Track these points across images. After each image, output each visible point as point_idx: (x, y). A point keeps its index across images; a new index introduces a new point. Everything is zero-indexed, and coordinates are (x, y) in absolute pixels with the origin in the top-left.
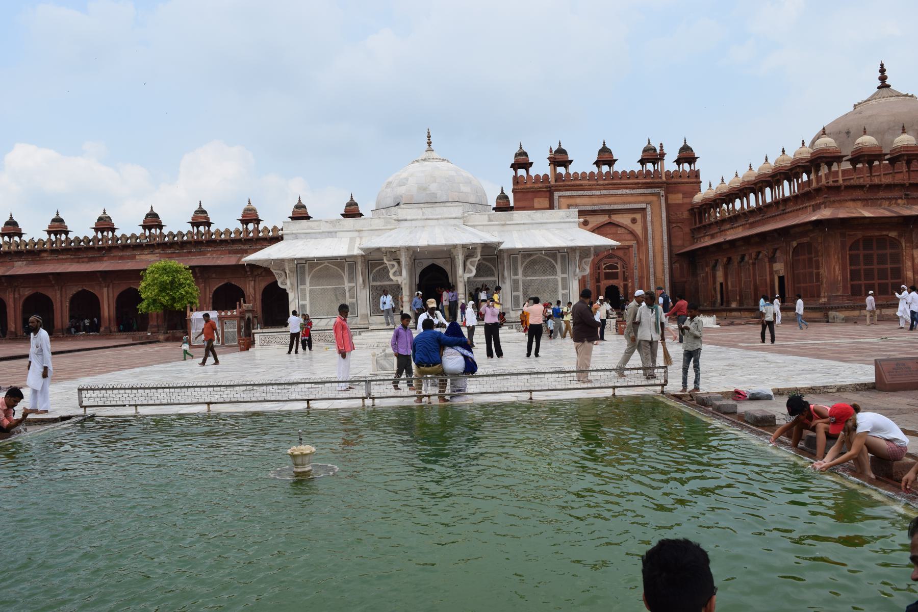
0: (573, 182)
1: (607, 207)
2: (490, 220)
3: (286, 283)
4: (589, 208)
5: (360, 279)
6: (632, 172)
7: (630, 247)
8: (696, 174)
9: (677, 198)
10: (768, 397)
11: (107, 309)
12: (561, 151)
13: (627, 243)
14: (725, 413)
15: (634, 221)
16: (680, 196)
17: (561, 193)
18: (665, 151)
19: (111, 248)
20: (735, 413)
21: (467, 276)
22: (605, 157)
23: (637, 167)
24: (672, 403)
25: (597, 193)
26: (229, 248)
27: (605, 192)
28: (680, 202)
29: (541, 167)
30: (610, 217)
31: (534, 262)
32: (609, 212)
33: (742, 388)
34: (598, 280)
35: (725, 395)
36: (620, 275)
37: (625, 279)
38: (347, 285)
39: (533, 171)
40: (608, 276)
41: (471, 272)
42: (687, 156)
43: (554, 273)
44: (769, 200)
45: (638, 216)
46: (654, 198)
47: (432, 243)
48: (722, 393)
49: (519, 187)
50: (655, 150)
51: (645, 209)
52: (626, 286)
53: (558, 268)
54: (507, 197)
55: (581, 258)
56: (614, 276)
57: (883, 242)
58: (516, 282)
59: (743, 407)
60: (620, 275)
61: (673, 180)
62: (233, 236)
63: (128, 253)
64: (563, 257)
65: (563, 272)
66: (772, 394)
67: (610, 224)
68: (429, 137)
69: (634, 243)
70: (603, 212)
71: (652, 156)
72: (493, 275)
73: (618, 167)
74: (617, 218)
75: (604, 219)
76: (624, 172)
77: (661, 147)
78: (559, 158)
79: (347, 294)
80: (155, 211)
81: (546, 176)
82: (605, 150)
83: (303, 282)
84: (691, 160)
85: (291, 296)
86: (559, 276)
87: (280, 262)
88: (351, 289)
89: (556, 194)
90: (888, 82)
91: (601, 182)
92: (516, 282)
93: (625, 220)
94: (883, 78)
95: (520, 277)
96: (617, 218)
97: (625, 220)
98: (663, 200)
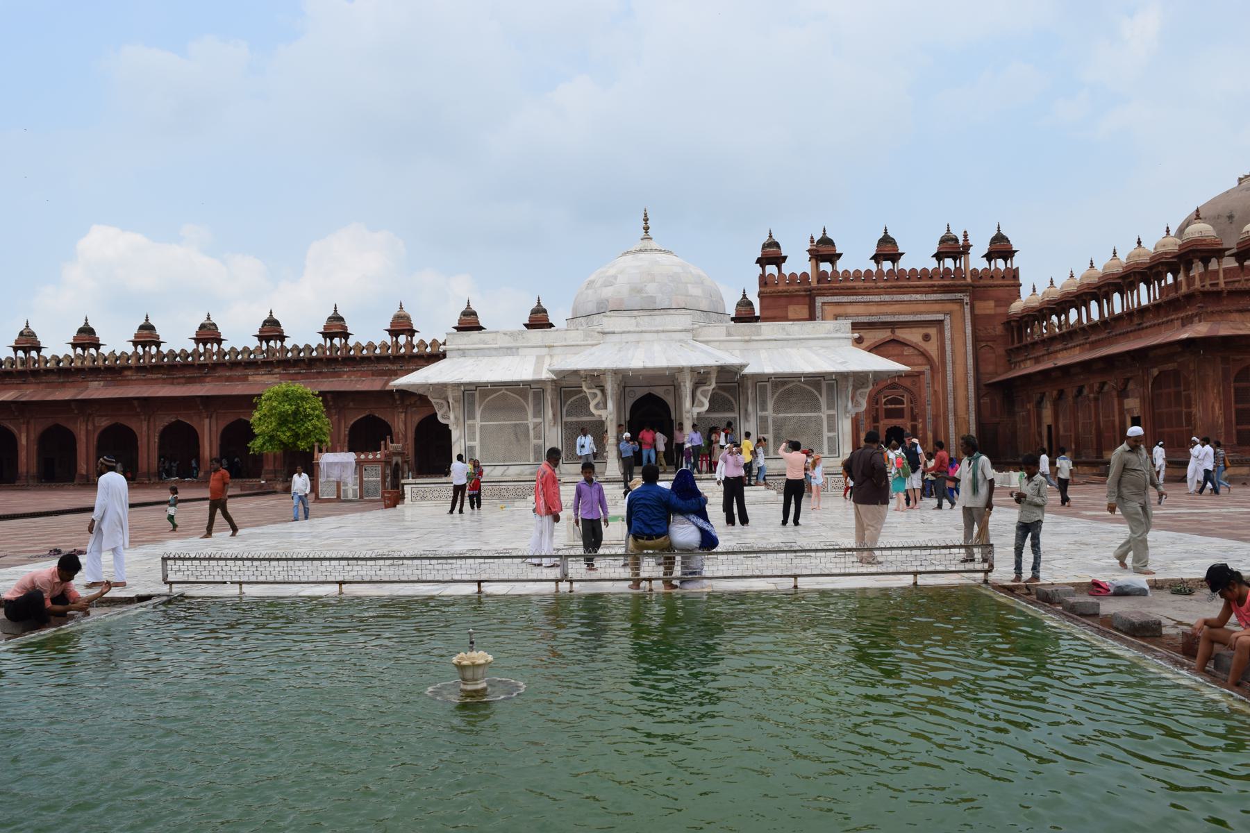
0: (842, 284)
1: (889, 319)
2: (729, 334)
3: (449, 417)
5: (549, 413)
6: (925, 270)
7: (921, 373)
8: (1014, 274)
9: (987, 307)
10: (1142, 592)
11: (209, 446)
12: (826, 241)
13: (917, 369)
14: (1082, 615)
15: (926, 338)
16: (992, 303)
17: (826, 299)
18: (971, 242)
19: (216, 366)
20: (1096, 615)
21: (696, 410)
22: (887, 250)
23: (932, 264)
24: (1002, 598)
25: (876, 298)
26: (373, 367)
27: (887, 298)
28: (992, 312)
29: (798, 263)
30: (893, 332)
31: (789, 392)
33: (1101, 578)
34: (876, 419)
35: (1079, 587)
36: (907, 413)
37: (914, 418)
38: (531, 421)
39: (787, 269)
40: (890, 414)
41: (702, 404)
42: (1001, 248)
43: (817, 408)
44: (1118, 310)
45: (932, 331)
46: (955, 307)
47: (650, 364)
48: (1073, 585)
50: (957, 240)
51: (942, 321)
53: (823, 401)
54: (750, 304)
55: (855, 388)
56: (899, 414)
58: (763, 420)
59: (1109, 607)
60: (907, 413)
61: (982, 282)
62: (378, 351)
63: (238, 373)
64: (830, 387)
65: (829, 408)
66: (1147, 587)
67: (893, 341)
68: (646, 220)
69: (926, 368)
71: (952, 248)
72: (732, 410)
73: (905, 264)
74: (903, 334)
75: (884, 335)
77: (966, 236)
78: (824, 251)
79: (532, 433)
80: (275, 316)
81: (805, 275)
82: (886, 240)
83: (471, 416)
84: (1008, 254)
85: (455, 435)
86: (824, 413)
87: (442, 388)
88: (536, 426)
91: (881, 284)
92: (763, 420)
93: (914, 336)
95: (770, 413)
96: (903, 334)
97: (914, 336)
98: (967, 309)
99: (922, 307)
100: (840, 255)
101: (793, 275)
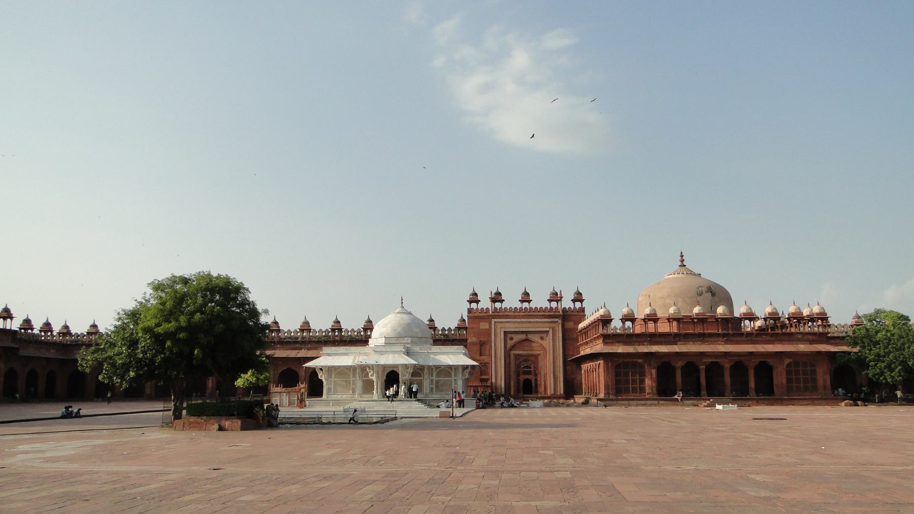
3: (321, 376)
8: (582, 310)
9: (570, 325)
22: (526, 298)
26: (292, 346)
31: (441, 371)
32: (526, 333)
34: (518, 376)
38: (352, 379)
39: (480, 306)
40: (525, 373)
42: (578, 298)
45: (544, 335)
52: (536, 380)
53: (453, 374)
56: (529, 373)
57: (635, 365)
58: (432, 380)
67: (527, 340)
70: (522, 332)
71: (555, 297)
73: (533, 305)
74: (531, 337)
75: (523, 337)
82: (526, 294)
84: (581, 301)
89: (493, 321)
90: (685, 263)
92: (432, 380)
94: (682, 261)
96: (531, 337)
99: (540, 325)
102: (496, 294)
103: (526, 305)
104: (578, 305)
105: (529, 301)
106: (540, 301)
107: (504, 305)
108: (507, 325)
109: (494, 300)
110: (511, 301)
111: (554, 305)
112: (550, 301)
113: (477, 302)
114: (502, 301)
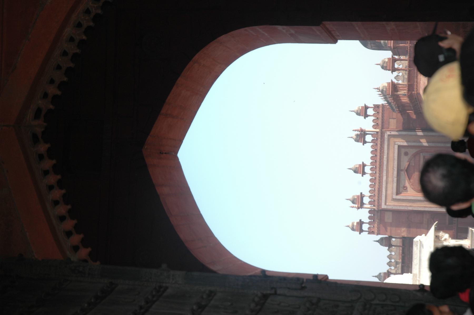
1: (395, 173)
4: (395, 185)
6: (372, 152)
8: (376, 107)
18: (359, 129)
22: (360, 170)
30: (402, 170)
42: (363, 112)
49: (376, 231)
54: (382, 239)
71: (361, 137)
73: (368, 161)
76: (372, 158)
77: (355, 131)
78: (358, 201)
81: (370, 212)
84: (366, 108)
91: (378, 175)
99: (391, 155)
100: (361, 193)
101: (370, 218)
102: (353, 202)
103: (367, 169)
104: (370, 112)
105: (364, 165)
106: (364, 153)
107: (367, 193)
108: (389, 192)
109: (361, 205)
110: (363, 185)
111: (369, 138)
112: (365, 142)
113: (361, 223)
114: (362, 196)
